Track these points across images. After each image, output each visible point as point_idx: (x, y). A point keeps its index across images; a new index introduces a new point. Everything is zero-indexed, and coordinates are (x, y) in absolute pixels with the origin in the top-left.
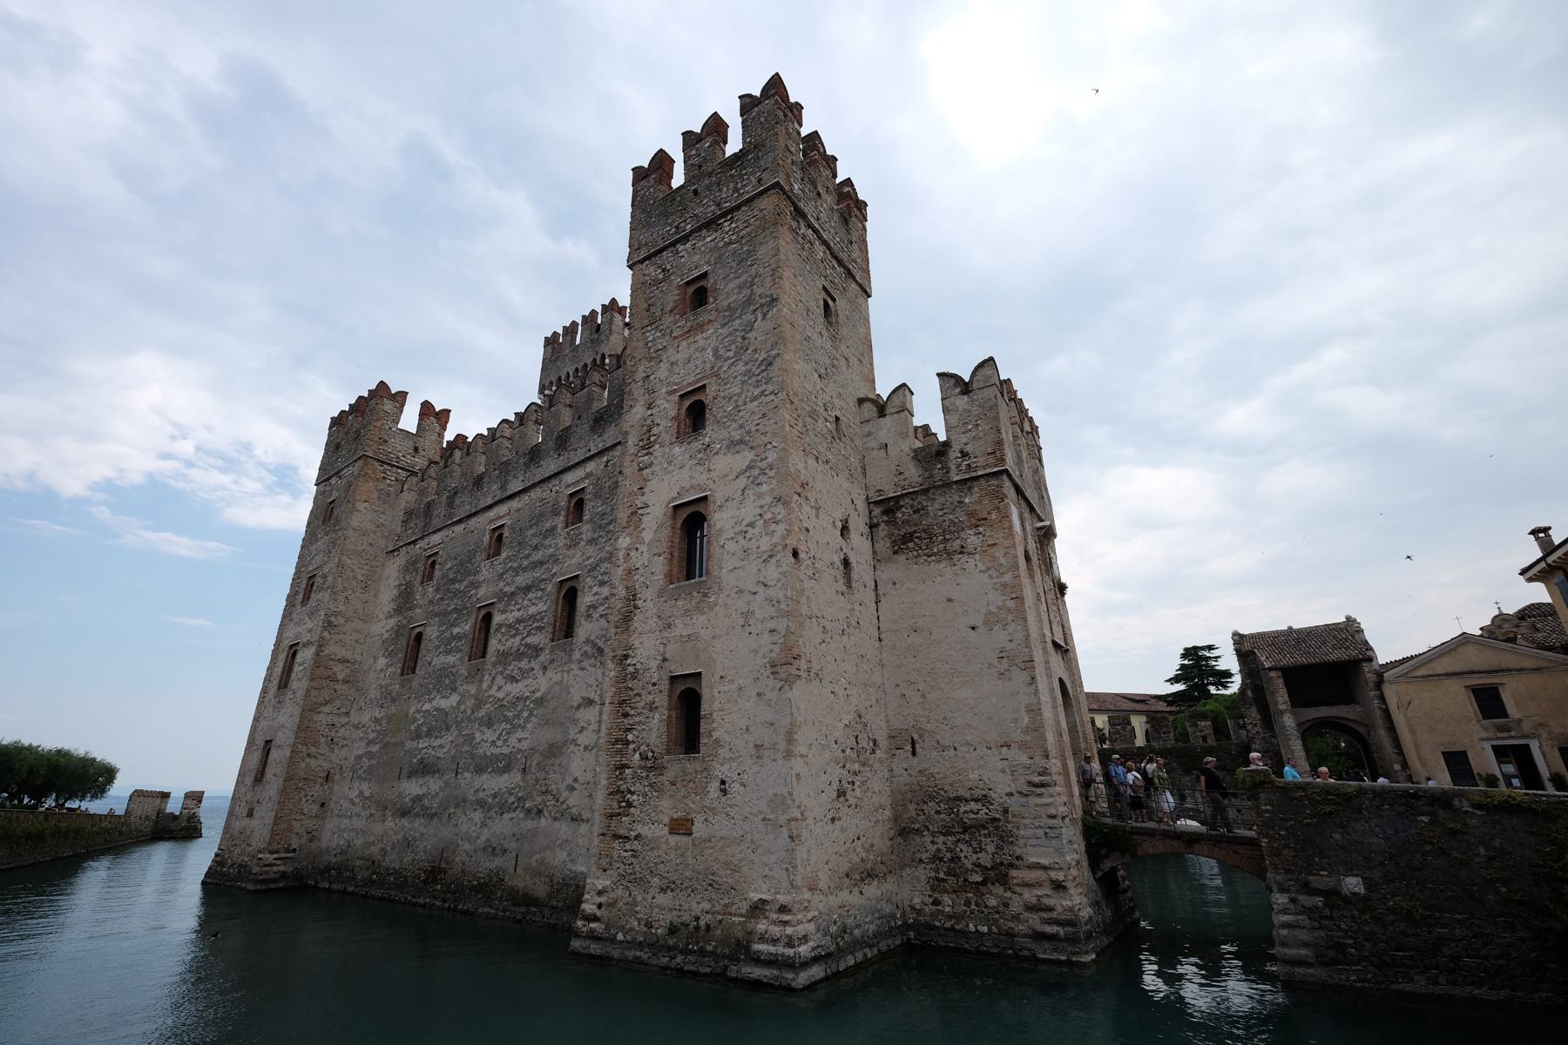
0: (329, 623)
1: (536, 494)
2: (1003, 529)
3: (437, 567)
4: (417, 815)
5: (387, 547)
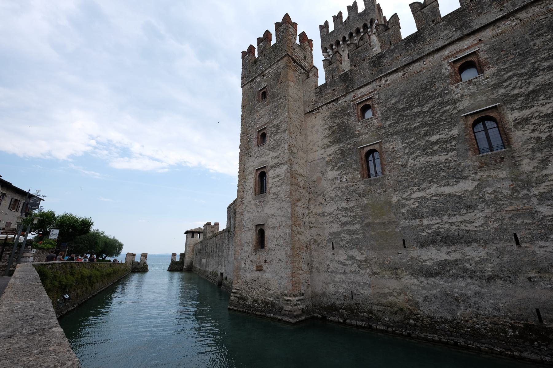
4: (455, 276)
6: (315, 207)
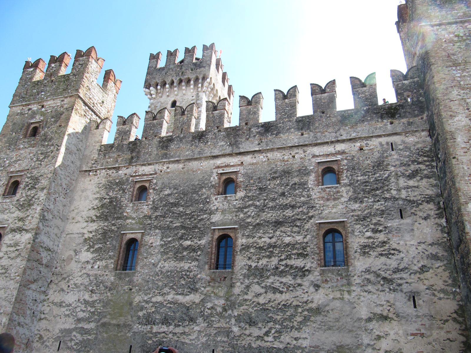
0: (44, 216)
1: (278, 155)
3: (151, 191)
6: (54, 294)
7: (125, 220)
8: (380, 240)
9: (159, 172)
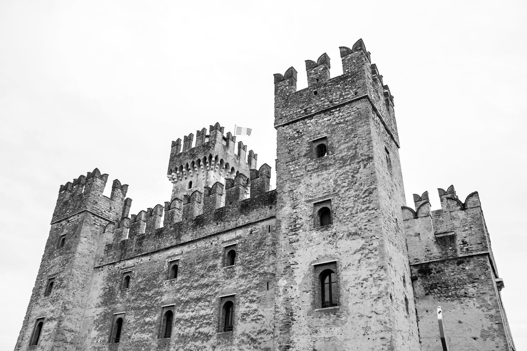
0: (65, 307)
1: (201, 244)
2: (488, 285)
3: (131, 280)
5: (95, 264)
7: (116, 304)
8: (253, 308)
9: (136, 264)
